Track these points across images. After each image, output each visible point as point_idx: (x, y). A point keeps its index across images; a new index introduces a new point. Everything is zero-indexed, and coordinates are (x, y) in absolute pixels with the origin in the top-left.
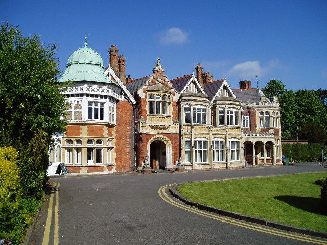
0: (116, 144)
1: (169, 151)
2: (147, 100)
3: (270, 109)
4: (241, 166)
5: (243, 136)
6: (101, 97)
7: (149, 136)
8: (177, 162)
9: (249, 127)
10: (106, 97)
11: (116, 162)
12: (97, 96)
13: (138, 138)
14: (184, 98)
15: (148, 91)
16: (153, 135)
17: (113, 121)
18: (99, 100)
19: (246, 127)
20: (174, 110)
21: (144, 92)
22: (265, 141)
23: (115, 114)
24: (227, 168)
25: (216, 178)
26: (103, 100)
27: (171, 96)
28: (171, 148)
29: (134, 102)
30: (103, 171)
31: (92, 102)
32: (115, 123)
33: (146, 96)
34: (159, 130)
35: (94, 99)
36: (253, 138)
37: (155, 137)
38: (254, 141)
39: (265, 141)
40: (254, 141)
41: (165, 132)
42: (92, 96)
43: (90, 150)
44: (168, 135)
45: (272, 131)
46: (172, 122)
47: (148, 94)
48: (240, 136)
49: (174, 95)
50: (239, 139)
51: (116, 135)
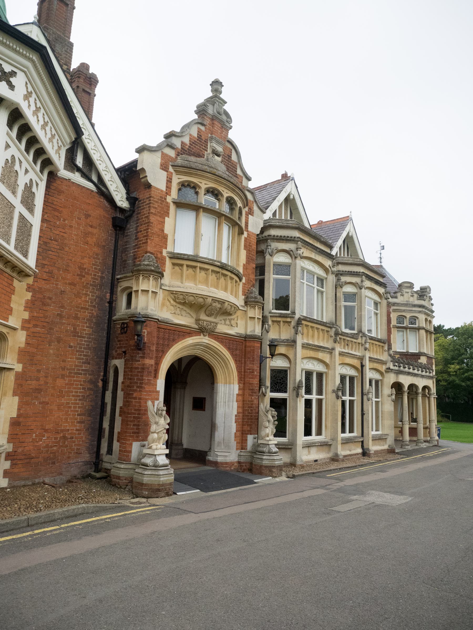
0: (25, 355)
1: (227, 396)
3: (420, 312)
4: (386, 447)
8: (250, 439)
13: (122, 337)
14: (273, 232)
15: (179, 169)
16: (180, 332)
17: (23, 246)
23: (36, 220)
24: (365, 453)
28: (235, 388)
29: (121, 200)
32: (31, 261)
33: (169, 181)
34: (203, 317)
37: (190, 341)
41: (223, 328)
44: (226, 340)
45: (423, 360)
51: (26, 315)
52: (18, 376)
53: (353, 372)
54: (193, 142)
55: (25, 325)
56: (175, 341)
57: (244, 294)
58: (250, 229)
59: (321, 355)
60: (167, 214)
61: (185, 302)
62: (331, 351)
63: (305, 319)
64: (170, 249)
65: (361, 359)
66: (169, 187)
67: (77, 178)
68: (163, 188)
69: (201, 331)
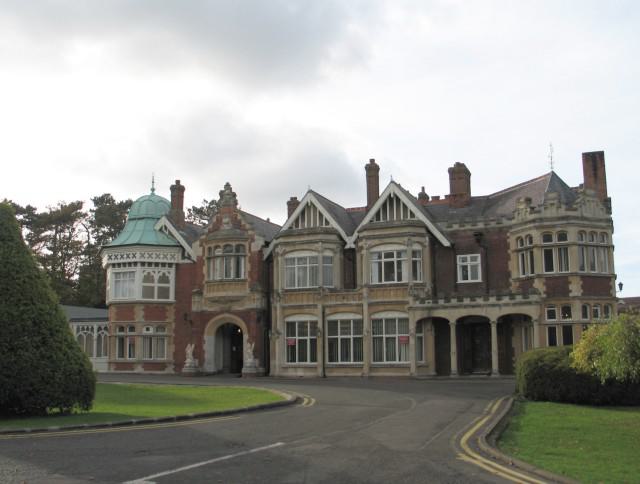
0: (175, 331)
2: (204, 258)
3: (530, 229)
5: (418, 304)
6: (130, 264)
7: (205, 317)
9: (480, 280)
10: (135, 263)
11: (174, 358)
12: (124, 264)
16: (212, 315)
18: (127, 269)
19: (470, 281)
20: (252, 268)
21: (201, 245)
22: (494, 315)
25: (116, 386)
26: (132, 269)
27: (247, 244)
30: (133, 369)
31: (119, 273)
35: (122, 269)
36: (445, 308)
38: (452, 315)
39: (494, 315)
40: (452, 315)
41: (237, 307)
42: (119, 265)
43: (122, 340)
46: (248, 290)
47: (206, 247)
48: (406, 307)
49: (253, 240)
50: (404, 312)
52: (175, 338)
53: (359, 317)
54: (214, 225)
55: (175, 321)
56: (211, 318)
57: (250, 287)
58: (253, 250)
59: (307, 310)
60: (203, 264)
61: (215, 301)
62: (315, 306)
63: (287, 291)
64: (206, 279)
65: (362, 305)
66: (204, 251)
67: (186, 261)
68: (200, 254)
69: (222, 312)
